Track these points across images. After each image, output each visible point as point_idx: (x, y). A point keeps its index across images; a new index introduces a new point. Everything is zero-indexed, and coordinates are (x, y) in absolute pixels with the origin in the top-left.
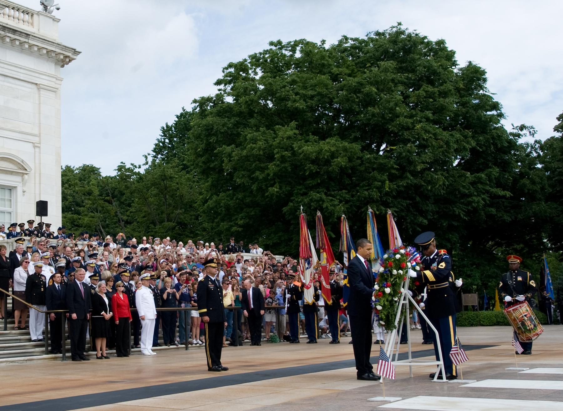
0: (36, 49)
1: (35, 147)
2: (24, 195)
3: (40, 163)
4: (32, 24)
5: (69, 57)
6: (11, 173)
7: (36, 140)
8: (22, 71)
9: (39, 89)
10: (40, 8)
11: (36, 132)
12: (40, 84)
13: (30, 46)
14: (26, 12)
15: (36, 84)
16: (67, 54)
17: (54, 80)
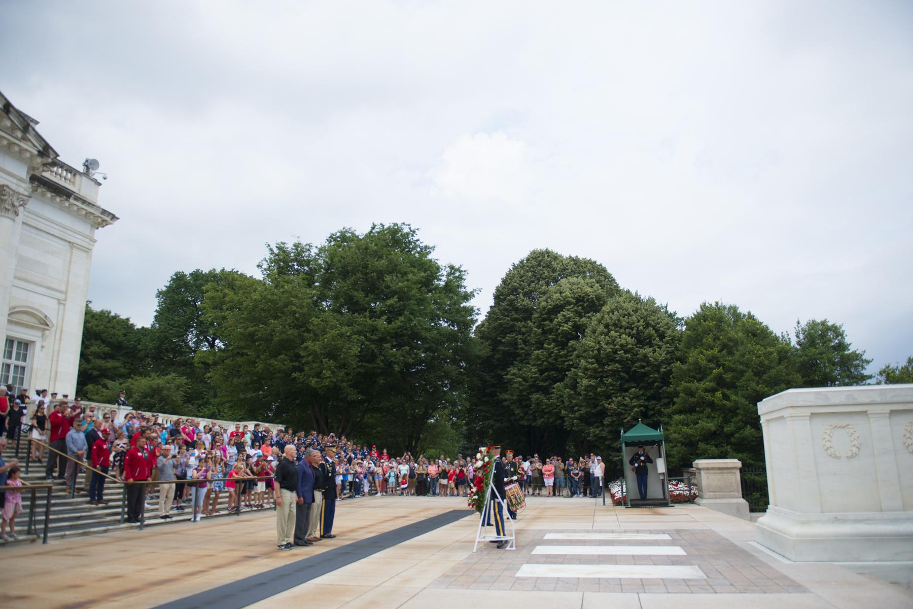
0: (75, 208)
1: (59, 303)
2: (42, 351)
3: (63, 321)
4: (74, 183)
5: (106, 221)
6: (32, 327)
7: (62, 296)
8: (57, 227)
9: (72, 248)
10: (81, 169)
11: (63, 288)
12: (73, 243)
13: (69, 205)
14: (70, 170)
15: (70, 242)
16: (105, 218)
17: (88, 240)
